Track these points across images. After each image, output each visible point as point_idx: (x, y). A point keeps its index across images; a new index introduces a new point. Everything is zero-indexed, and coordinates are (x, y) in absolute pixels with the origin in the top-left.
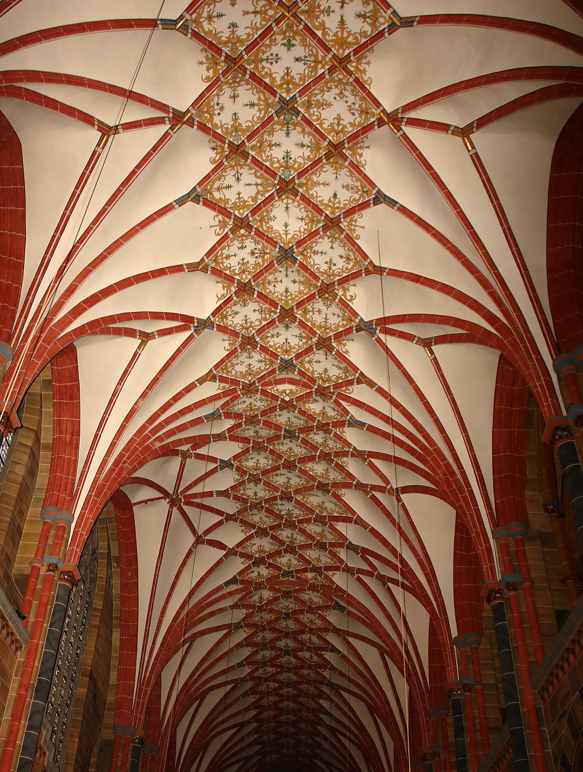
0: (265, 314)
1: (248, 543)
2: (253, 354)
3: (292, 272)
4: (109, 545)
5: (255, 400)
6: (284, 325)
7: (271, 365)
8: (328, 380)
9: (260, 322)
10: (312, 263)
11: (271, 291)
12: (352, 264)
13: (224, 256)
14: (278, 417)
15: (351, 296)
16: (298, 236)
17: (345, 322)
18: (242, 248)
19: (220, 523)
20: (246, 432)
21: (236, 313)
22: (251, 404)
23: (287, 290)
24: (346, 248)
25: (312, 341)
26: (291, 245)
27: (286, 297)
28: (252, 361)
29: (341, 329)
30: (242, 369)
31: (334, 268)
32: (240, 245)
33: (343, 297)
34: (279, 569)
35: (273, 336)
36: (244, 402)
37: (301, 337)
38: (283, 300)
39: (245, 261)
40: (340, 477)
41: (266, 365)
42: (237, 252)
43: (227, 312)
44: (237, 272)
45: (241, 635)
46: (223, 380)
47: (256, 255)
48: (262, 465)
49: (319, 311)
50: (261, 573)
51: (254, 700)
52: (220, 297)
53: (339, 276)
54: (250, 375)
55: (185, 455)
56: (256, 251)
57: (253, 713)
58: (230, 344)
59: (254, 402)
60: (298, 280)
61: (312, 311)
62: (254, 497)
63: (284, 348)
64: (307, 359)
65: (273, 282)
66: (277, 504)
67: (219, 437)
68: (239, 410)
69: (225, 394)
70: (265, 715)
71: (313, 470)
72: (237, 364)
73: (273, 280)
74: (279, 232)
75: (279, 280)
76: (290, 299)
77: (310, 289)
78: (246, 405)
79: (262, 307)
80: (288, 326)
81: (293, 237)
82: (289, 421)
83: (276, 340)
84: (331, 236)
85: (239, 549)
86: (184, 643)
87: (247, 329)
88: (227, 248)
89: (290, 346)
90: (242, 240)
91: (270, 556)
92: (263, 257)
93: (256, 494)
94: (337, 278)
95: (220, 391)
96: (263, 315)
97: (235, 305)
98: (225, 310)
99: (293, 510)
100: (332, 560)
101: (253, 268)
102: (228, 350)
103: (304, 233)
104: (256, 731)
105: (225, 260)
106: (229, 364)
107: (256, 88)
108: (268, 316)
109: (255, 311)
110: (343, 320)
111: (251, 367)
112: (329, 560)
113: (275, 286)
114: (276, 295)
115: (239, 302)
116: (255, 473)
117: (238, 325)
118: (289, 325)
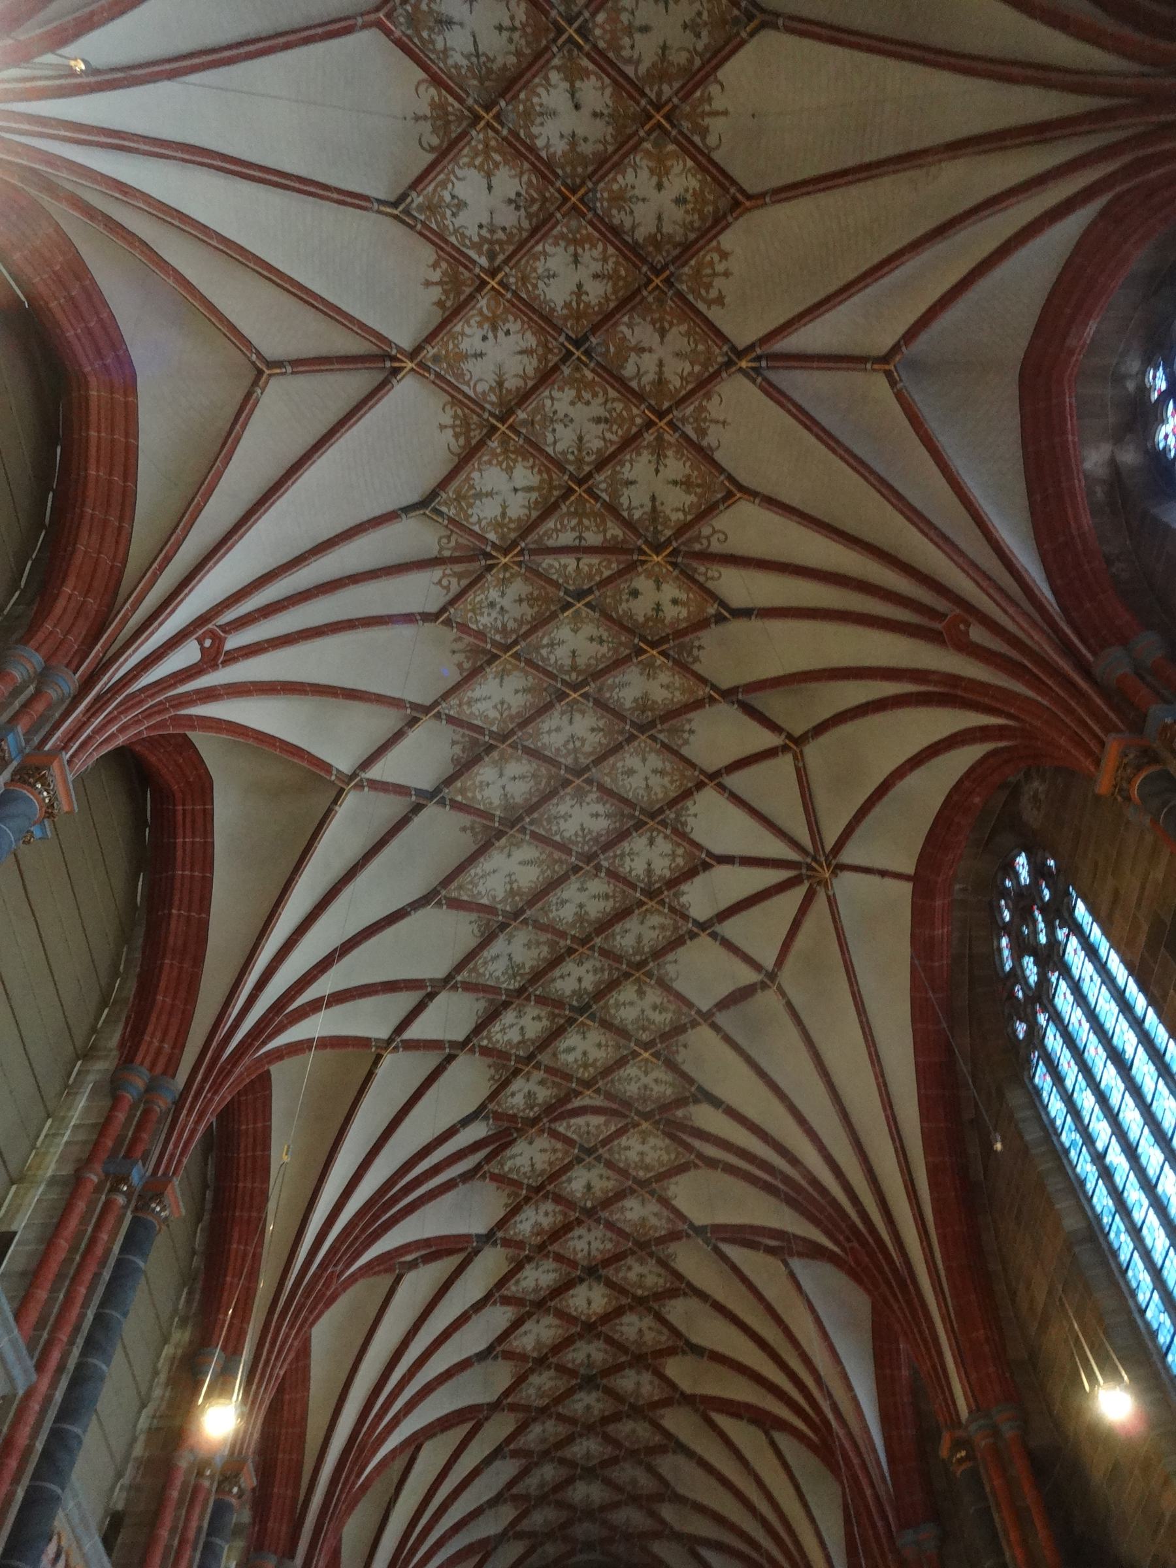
18: (641, 1276)
22: (646, 1073)
41: (619, 1144)
50: (651, 583)
62: (655, 834)
64: (560, 1155)
66: (608, 816)
93: (651, 842)
99: (572, 806)
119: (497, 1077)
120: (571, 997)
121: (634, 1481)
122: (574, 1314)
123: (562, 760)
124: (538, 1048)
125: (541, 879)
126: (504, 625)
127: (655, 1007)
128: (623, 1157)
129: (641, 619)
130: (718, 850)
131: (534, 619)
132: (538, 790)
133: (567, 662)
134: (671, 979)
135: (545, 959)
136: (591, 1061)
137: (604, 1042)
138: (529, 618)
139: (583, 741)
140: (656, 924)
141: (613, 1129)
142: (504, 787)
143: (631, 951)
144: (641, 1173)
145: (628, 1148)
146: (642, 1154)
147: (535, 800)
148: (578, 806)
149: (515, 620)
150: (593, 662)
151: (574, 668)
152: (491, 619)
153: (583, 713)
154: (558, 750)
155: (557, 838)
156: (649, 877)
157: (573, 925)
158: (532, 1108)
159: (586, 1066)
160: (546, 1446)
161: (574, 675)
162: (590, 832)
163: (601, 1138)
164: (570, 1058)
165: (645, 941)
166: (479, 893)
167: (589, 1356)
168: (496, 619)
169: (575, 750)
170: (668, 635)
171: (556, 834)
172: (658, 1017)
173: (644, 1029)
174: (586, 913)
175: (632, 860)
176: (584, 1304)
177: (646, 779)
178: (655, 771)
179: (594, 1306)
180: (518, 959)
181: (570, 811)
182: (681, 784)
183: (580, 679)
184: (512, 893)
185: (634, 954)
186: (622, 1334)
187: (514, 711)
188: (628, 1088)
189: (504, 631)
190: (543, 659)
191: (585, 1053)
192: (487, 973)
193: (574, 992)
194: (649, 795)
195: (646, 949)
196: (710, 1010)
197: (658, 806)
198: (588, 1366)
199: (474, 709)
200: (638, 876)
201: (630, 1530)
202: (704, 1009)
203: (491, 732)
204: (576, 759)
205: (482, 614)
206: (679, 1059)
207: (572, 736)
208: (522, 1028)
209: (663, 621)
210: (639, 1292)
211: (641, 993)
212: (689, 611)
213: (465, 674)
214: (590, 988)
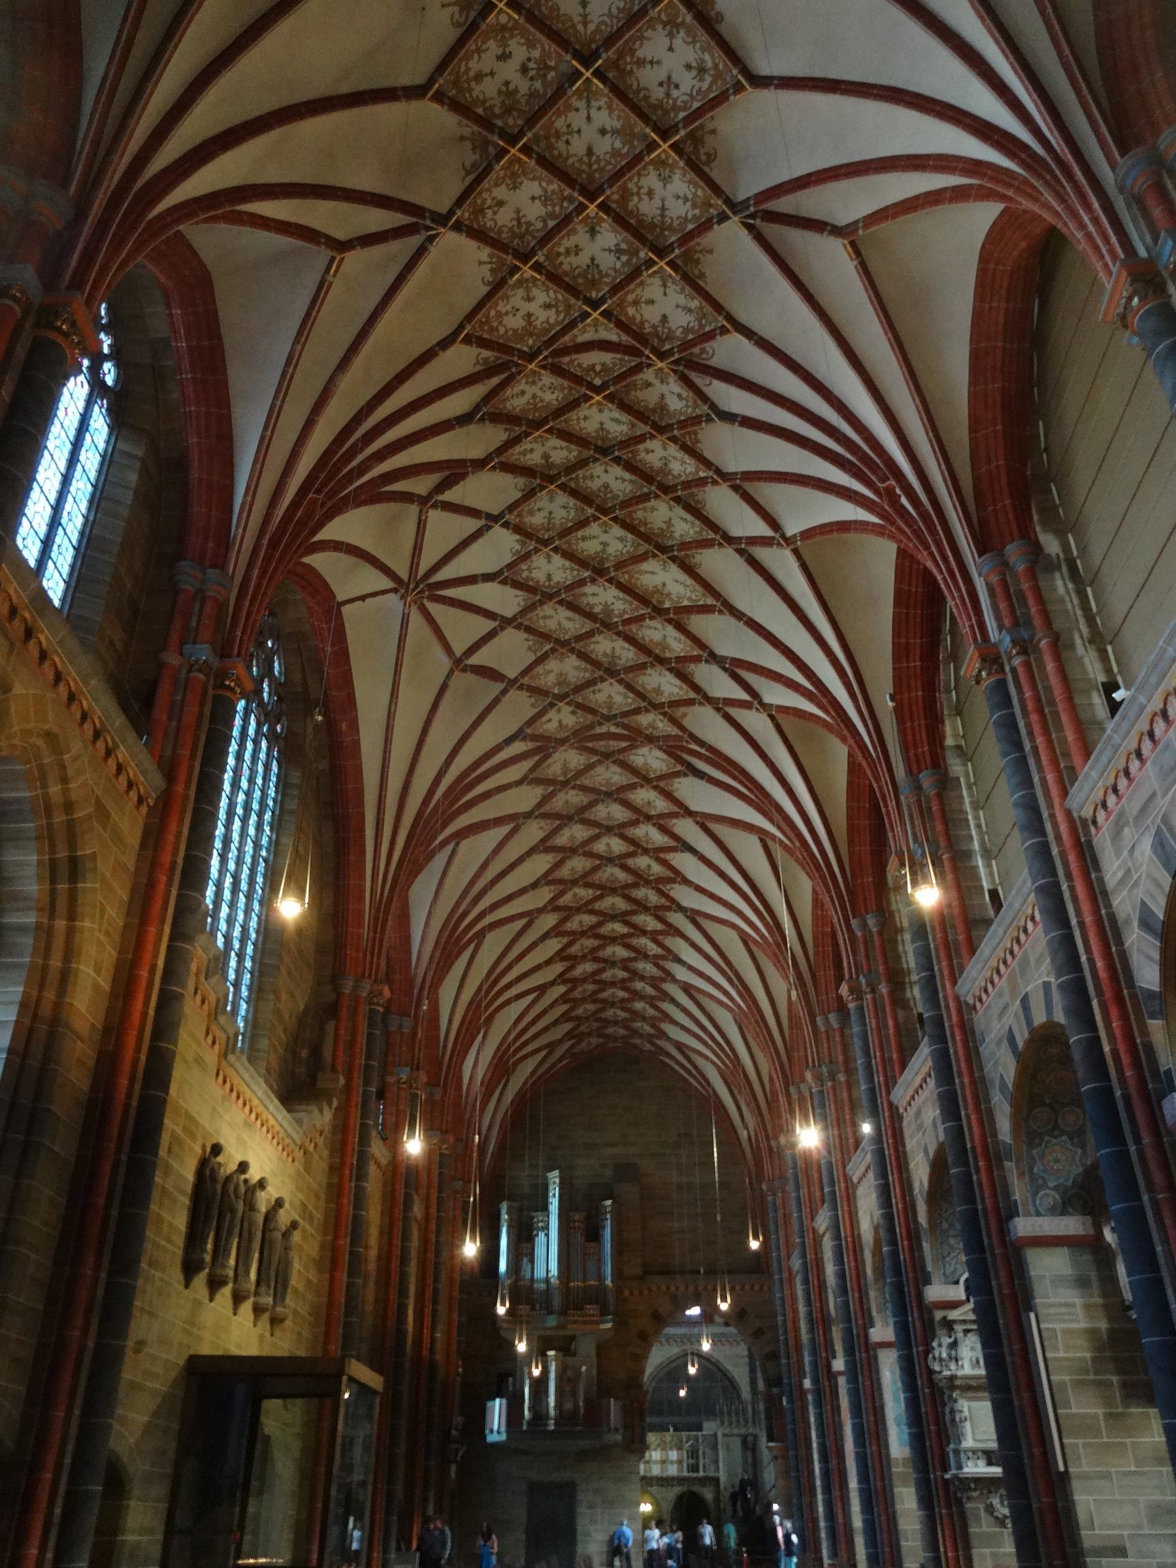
0: (553, 205)
1: (540, 669)
2: (535, 292)
4: (304, 678)
7: (567, 313)
8: (670, 337)
9: (545, 221)
10: (635, 87)
11: (560, 155)
12: (708, 79)
13: (472, 74)
14: (582, 422)
15: (708, 155)
16: (606, 25)
17: (697, 211)
18: (504, 57)
19: (491, 635)
20: (528, 456)
21: (501, 204)
22: (534, 396)
23: (590, 152)
24: (698, 45)
25: (639, 258)
26: (594, 46)
27: (590, 165)
28: (533, 307)
29: (690, 227)
30: (515, 322)
31: (675, 93)
32: (500, 51)
33: (693, 157)
34: (593, 711)
35: (568, 252)
36: (523, 393)
37: (618, 251)
38: (583, 171)
39: (512, 87)
40: (692, 532)
41: (558, 313)
42: (498, 66)
43: (484, 201)
44: (497, 111)
45: (534, 831)
46: (483, 343)
47: (532, 73)
48: (557, 522)
49: (650, 193)
50: (564, 722)
51: (559, 947)
52: (468, 165)
53: (685, 109)
54: (531, 335)
55: (424, 501)
56: (532, 65)
57: (559, 968)
58: (492, 270)
59: (539, 393)
60: (609, 128)
61: (638, 194)
63: (590, 277)
65: (564, 134)
66: (585, 595)
67: (479, 464)
68: (514, 408)
69: (488, 372)
70: (578, 971)
71: (646, 524)
72: (507, 313)
73: (564, 129)
74: (571, 20)
75: (576, 129)
76: (596, 170)
77: (632, 146)
78: (528, 396)
79: (545, 191)
81: (598, 30)
83: (573, 259)
84: (668, 23)
85: (526, 680)
86: (444, 844)
87: (522, 237)
88: (476, 55)
89: (600, 272)
90: (503, 38)
91: (578, 689)
92: (545, 75)
93: (549, 577)
94: (682, 115)
95: (479, 368)
96: (550, 208)
97: (497, 185)
98: (480, 193)
100: (681, 688)
101: (527, 102)
102: (489, 283)
103: (617, 17)
104: (564, 998)
105: (473, 84)
106: (493, 313)
108: (557, 209)
109: (533, 198)
110: (694, 206)
111: (533, 318)
112: (676, 690)
113: (568, 142)
114: (570, 161)
115: (503, 178)
116: (546, 537)
117: (506, 230)
145: (547, 306)
146: (529, 299)
153: (605, 655)
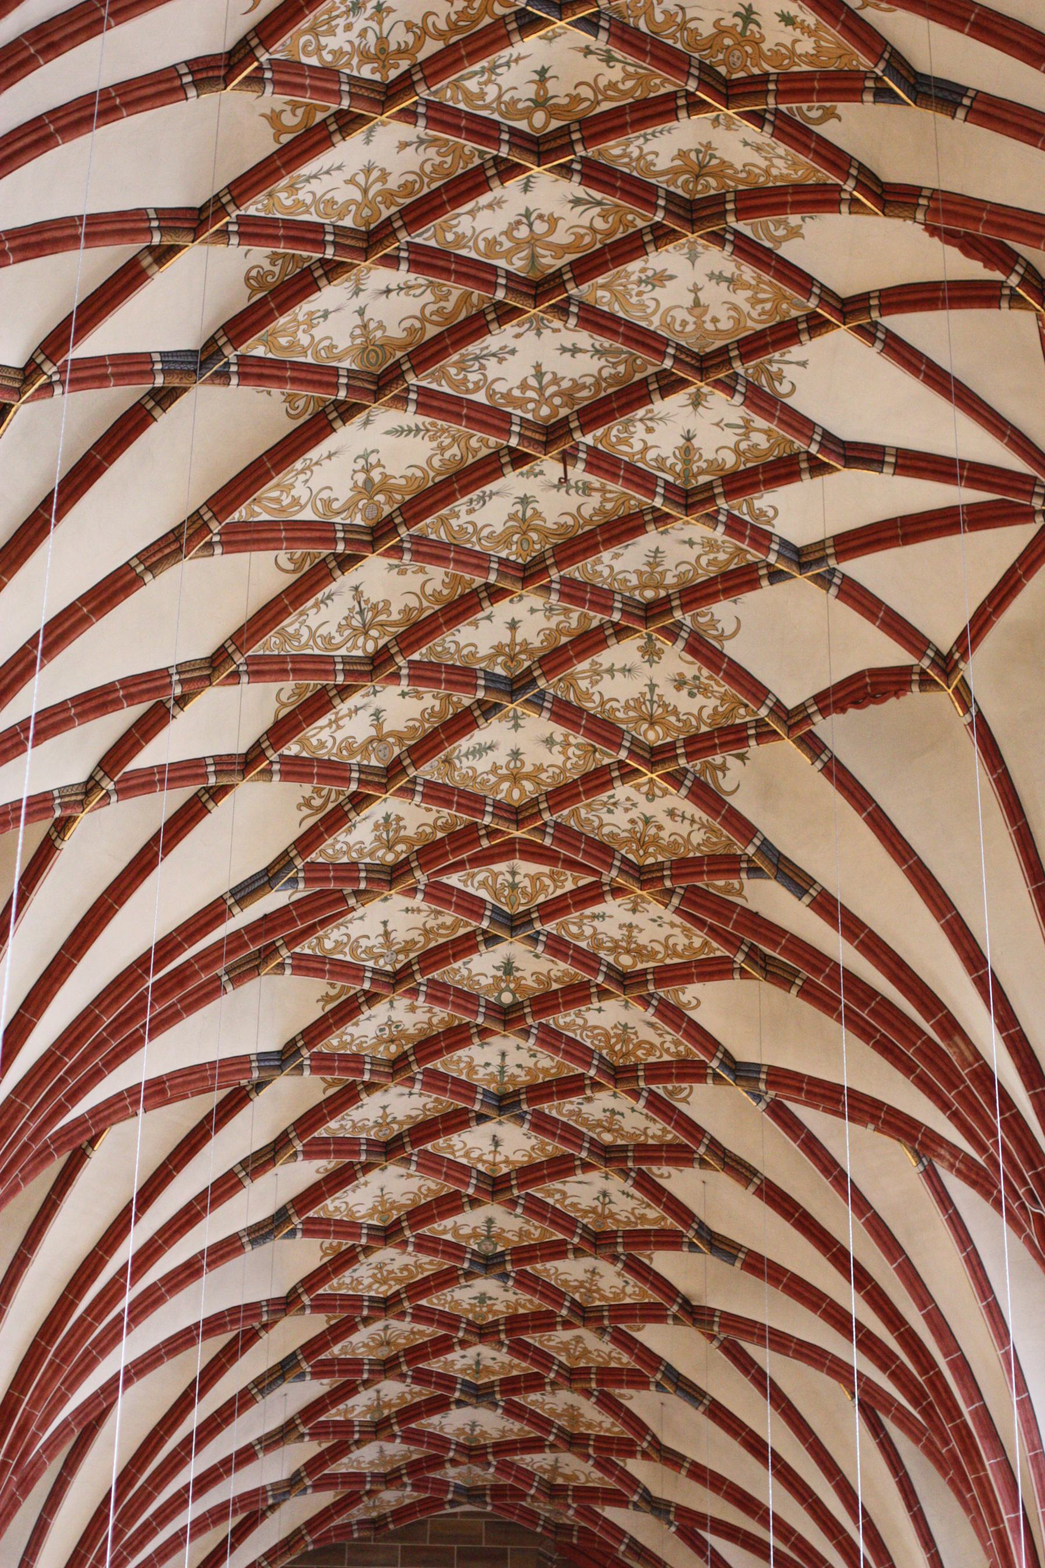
2: (618, 935)
3: (487, 1064)
5: (634, 805)
6: (518, 974)
59: (640, 798)
80: (505, 973)
82: (516, 717)
107: (549, 1276)
111: (630, 906)
118: (500, 973)
119: (317, 802)
120: (491, 658)
121: (573, 1413)
122: (464, 1161)
123: (501, 263)
124: (411, 750)
125: (436, 462)
126: (382, 40)
127: (680, 683)
128: (588, 931)
129: (706, 30)
130: (848, 432)
131: (454, 28)
132: (439, 312)
133: (530, 91)
134: (721, 637)
135: (436, 596)
136: (528, 768)
137: (558, 738)
138: (443, 26)
139: (553, 222)
140: (697, 539)
141: (569, 886)
142: (361, 312)
143: (634, 580)
144: (626, 960)
147: (432, 331)
148: (532, 334)
149: (409, 26)
150: (586, 92)
151: (540, 102)
152: (353, 35)
154: (492, 243)
155: (480, 397)
156: (687, 461)
157: (504, 540)
158: (390, 848)
159: (515, 778)
160: (383, 1353)
161: (539, 118)
162: (556, 380)
163: (541, 899)
164: (482, 765)
165: (669, 563)
166: (296, 501)
167: (490, 1221)
168: (363, 33)
169: (533, 241)
170: (765, 77)
171: (477, 388)
172: (686, 704)
173: (652, 722)
174: (537, 514)
175: (650, 430)
176: (487, 1146)
177: (696, 290)
178: (717, 277)
179: (506, 1150)
180: (374, 594)
181: (512, 343)
182: (776, 309)
183: (555, 124)
184: (369, 488)
185: (643, 587)
186: (564, 1194)
187: (393, 183)
188: (607, 818)
189: (382, 55)
190: (469, 96)
191: (516, 754)
192: (305, 632)
193: (499, 650)
194: (699, 324)
195: (670, 580)
196: (802, 707)
197: (718, 344)
198: (488, 1237)
199: (301, 195)
200: (661, 460)
201: (560, 1481)
202: (790, 704)
203: (339, 231)
204: (533, 257)
205: (332, 32)
206: (726, 783)
207: (528, 214)
208: (377, 714)
209: (757, 43)
210: (607, 1138)
211: (651, 653)
212: (818, 47)
213: (285, 139)
214: (536, 642)
